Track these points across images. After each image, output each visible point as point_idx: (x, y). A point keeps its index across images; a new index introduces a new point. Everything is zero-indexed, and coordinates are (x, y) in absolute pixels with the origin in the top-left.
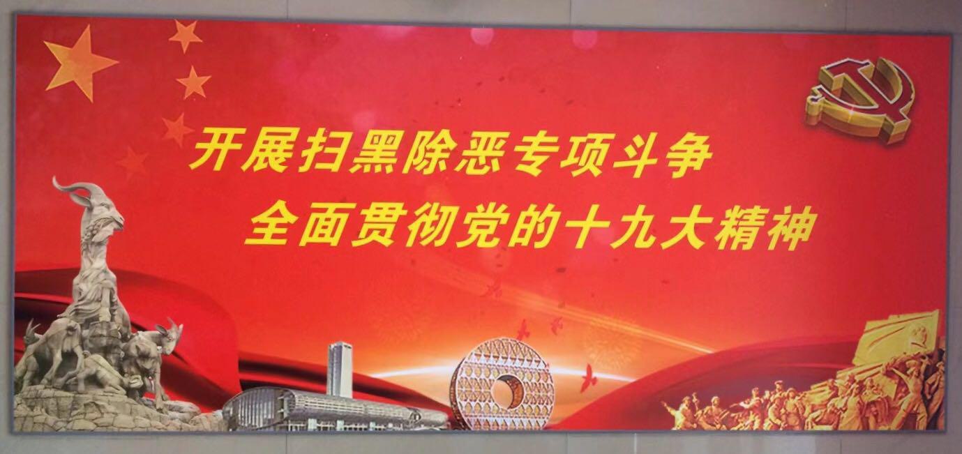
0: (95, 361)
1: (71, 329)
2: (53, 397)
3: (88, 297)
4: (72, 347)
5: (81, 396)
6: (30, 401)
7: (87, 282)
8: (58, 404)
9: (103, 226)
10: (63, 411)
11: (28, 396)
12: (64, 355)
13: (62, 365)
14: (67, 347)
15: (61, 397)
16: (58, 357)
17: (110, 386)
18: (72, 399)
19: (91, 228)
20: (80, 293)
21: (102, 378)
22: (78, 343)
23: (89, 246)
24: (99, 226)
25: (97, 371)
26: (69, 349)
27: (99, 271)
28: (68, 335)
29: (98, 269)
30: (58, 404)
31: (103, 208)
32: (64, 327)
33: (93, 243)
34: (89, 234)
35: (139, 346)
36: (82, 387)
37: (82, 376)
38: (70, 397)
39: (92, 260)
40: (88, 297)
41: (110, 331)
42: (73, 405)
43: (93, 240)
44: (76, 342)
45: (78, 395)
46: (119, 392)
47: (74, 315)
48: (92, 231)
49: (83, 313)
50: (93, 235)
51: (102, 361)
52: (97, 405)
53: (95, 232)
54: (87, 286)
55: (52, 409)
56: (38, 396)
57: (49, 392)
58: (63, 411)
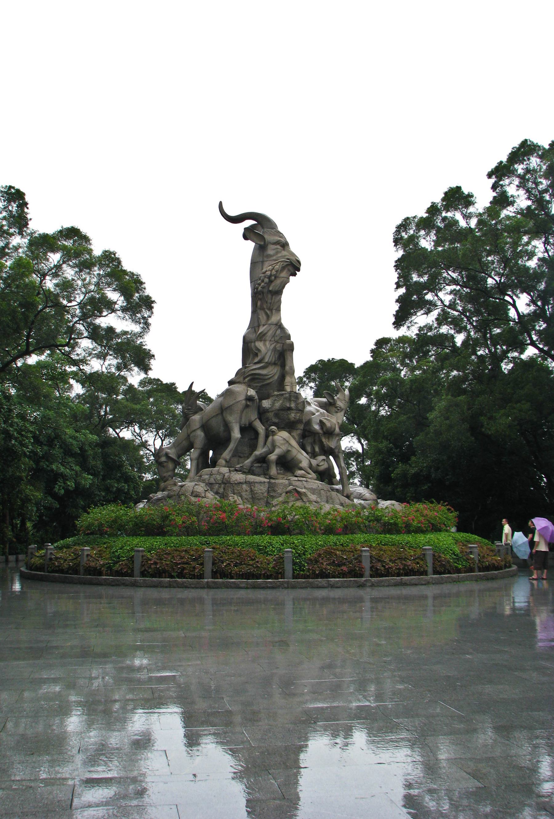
0: (284, 439)
1: (249, 399)
2: (246, 482)
5: (277, 481)
6: (217, 486)
7: (265, 341)
8: (252, 491)
10: (259, 500)
11: (212, 481)
12: (243, 430)
14: (245, 421)
15: (255, 483)
16: (236, 434)
17: (301, 469)
18: (267, 485)
19: (268, 273)
21: (293, 459)
22: (256, 417)
24: (277, 271)
25: (288, 451)
26: (247, 424)
28: (247, 406)
30: (252, 491)
33: (270, 291)
34: (266, 280)
35: (325, 421)
36: (274, 470)
37: (273, 457)
39: (268, 312)
41: (298, 404)
42: (268, 492)
43: (270, 289)
45: (273, 481)
46: (310, 476)
47: (249, 380)
48: (269, 277)
50: (271, 282)
54: (265, 345)
55: (246, 497)
57: (238, 477)
58: (259, 500)
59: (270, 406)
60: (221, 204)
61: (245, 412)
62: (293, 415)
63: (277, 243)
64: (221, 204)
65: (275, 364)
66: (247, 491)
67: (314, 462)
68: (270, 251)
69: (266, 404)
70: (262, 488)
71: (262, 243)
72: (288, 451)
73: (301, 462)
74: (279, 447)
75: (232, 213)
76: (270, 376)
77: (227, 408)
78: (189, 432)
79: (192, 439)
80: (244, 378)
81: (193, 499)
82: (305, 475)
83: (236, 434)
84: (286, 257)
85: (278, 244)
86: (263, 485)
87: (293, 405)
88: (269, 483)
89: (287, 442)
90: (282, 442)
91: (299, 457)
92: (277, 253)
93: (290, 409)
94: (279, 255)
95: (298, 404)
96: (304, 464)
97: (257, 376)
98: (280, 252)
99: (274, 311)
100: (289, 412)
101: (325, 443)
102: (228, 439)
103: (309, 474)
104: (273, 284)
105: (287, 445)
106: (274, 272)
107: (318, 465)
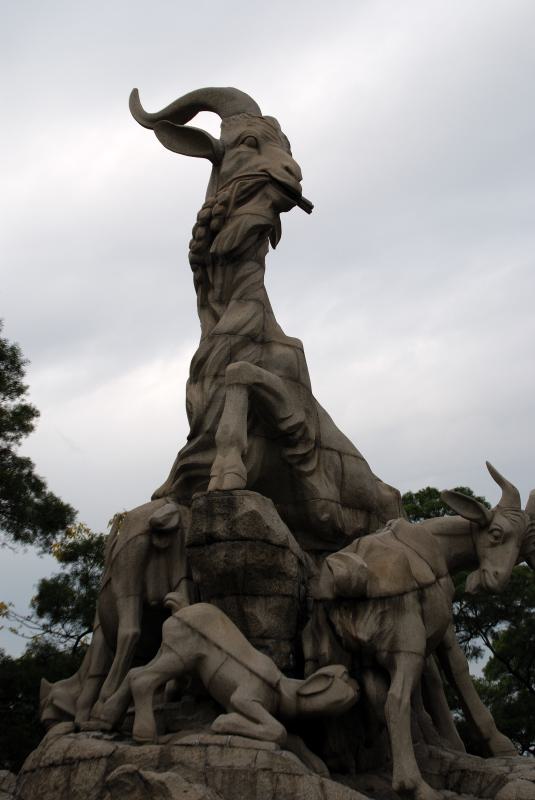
3: (207, 426)
7: (204, 377)
9: (240, 203)
23: (209, 270)
24: (225, 204)
25: (200, 659)
27: (237, 339)
29: (232, 333)
31: (243, 148)
39: (217, 308)
40: (207, 426)
41: (234, 522)
51: (223, 631)
52: (146, 782)
53: (214, 223)
54: (202, 388)
60: (135, 95)
61: (152, 566)
62: (222, 554)
63: (240, 141)
64: (135, 95)
67: (289, 686)
68: (225, 167)
71: (210, 152)
72: (200, 659)
73: (234, 688)
74: (170, 649)
75: (154, 105)
82: (237, 726)
84: (260, 168)
85: (243, 142)
86: (94, 766)
87: (220, 528)
89: (194, 630)
90: (179, 633)
91: (232, 672)
92: (240, 162)
93: (211, 539)
94: (244, 168)
95: (234, 522)
96: (245, 692)
97: (193, 473)
98: (247, 160)
100: (212, 547)
101: (338, 627)
103: (257, 721)
104: (217, 238)
105: (193, 640)
106: (217, 208)
107: (299, 695)
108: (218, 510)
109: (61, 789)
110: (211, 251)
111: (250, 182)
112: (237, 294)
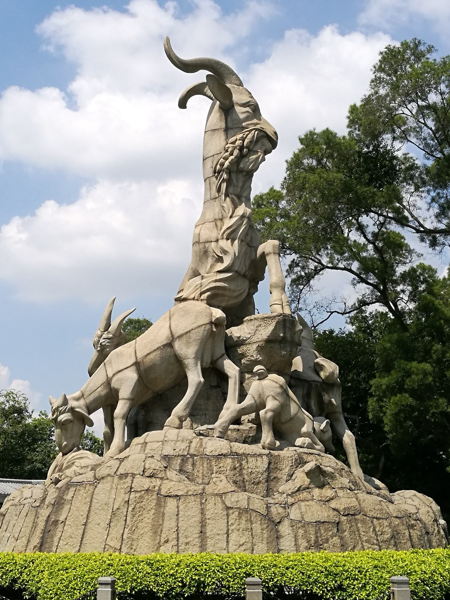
1: (217, 323)
4: (212, 356)
13: (202, 392)
16: (195, 377)
18: (265, 459)
20: (220, 260)
22: (224, 351)
23: (234, 176)
26: (209, 361)
32: (206, 320)
34: (236, 152)
38: (261, 455)
44: (221, 349)
47: (208, 297)
49: (223, 295)
56: (192, 451)
59: (249, 336)
65: (244, 276)
66: (235, 469)
69: (235, 332)
70: (259, 463)
71: (227, 102)
76: (237, 293)
77: (180, 337)
78: (110, 375)
79: (114, 384)
80: (201, 294)
81: (146, 483)
83: (195, 377)
86: (259, 459)
88: (269, 455)
97: (220, 292)
99: (244, 199)
102: (182, 383)
108: (288, 325)
109: (238, 469)
110: (241, 166)
111: (262, 134)
112: (245, 194)
